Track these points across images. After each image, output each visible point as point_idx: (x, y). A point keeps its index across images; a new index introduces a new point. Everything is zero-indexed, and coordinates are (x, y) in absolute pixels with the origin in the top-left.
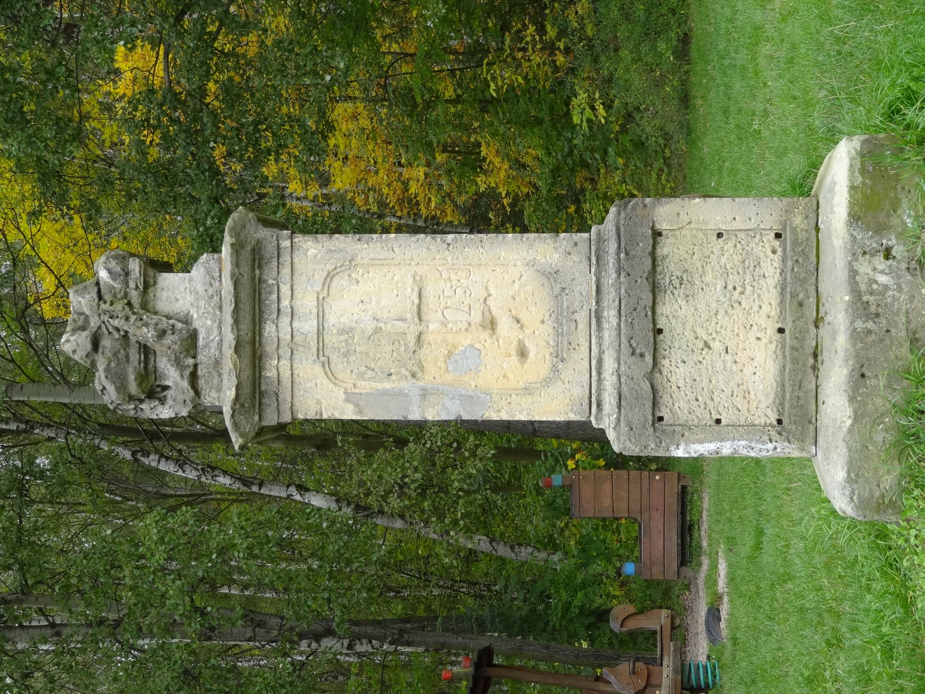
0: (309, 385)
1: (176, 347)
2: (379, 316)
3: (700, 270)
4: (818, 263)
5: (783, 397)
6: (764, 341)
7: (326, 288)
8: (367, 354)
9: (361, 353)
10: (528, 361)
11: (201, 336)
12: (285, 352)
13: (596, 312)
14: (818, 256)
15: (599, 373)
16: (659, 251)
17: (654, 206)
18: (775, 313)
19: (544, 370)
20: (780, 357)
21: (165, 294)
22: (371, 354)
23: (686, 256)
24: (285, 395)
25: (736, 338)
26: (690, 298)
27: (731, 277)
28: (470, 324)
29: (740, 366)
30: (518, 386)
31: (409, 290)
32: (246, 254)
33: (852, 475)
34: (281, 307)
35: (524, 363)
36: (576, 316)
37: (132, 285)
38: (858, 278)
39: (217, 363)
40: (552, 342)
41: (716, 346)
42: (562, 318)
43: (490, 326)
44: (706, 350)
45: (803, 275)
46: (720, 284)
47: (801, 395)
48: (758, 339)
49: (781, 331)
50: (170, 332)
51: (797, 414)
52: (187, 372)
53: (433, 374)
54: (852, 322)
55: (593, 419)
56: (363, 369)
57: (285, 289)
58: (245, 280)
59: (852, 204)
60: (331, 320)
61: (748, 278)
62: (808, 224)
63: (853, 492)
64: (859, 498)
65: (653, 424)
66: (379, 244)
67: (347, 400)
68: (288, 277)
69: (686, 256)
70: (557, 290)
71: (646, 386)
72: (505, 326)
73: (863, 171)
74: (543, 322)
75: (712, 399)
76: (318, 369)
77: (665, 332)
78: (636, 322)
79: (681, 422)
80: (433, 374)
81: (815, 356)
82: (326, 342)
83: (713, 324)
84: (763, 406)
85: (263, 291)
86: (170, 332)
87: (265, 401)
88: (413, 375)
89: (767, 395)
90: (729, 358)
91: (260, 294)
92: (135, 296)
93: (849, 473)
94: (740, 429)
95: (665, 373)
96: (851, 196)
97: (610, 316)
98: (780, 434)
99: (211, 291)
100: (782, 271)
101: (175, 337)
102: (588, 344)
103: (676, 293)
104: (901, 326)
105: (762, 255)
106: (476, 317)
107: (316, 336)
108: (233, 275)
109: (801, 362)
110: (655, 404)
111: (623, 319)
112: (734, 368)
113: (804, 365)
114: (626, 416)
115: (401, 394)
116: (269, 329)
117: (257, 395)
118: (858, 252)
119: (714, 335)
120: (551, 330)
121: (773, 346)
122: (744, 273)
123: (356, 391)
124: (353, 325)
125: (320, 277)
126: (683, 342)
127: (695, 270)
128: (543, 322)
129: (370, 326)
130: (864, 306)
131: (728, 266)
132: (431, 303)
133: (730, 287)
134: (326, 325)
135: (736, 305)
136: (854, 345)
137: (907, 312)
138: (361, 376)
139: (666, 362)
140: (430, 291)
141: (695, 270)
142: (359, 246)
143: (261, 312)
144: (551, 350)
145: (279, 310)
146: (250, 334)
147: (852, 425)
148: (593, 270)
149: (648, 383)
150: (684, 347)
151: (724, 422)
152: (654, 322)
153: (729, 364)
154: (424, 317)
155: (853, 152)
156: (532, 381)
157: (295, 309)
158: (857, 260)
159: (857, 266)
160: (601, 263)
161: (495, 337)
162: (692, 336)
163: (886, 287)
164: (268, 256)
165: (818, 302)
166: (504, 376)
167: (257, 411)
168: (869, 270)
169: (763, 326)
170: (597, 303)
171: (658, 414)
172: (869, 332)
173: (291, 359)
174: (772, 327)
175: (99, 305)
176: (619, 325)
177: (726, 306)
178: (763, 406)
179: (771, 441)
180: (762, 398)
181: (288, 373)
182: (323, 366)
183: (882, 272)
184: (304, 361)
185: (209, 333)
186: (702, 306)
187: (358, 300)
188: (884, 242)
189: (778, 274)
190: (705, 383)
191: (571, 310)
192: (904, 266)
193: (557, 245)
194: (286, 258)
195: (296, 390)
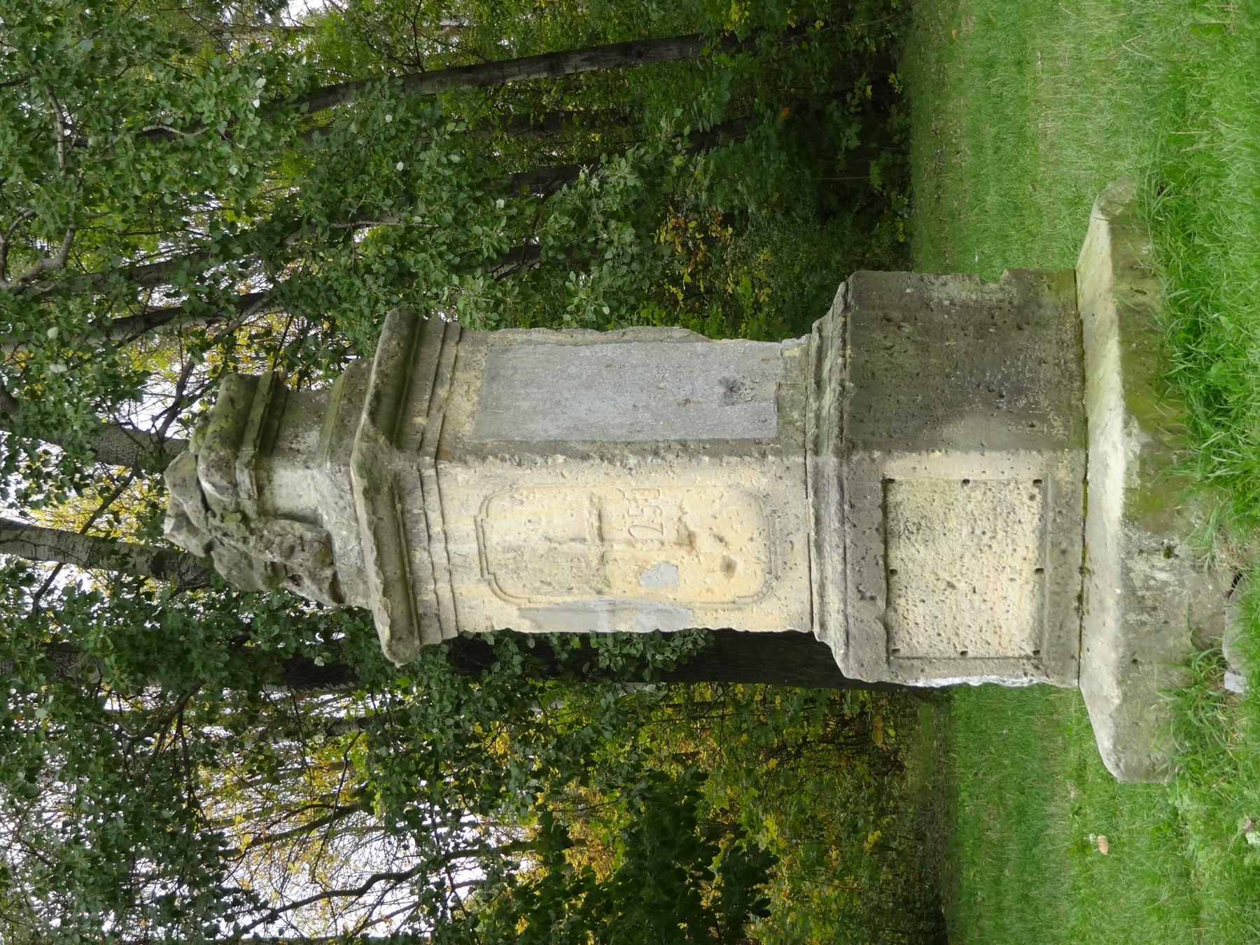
0: (474, 603)
1: (309, 564)
2: (551, 535)
3: (942, 516)
4: (1085, 514)
5: (1041, 632)
6: (1019, 582)
7: (484, 511)
8: (542, 570)
9: (533, 569)
10: (736, 575)
11: (337, 545)
12: (442, 575)
13: (816, 541)
14: (1085, 508)
15: (822, 597)
16: (891, 498)
17: (884, 460)
18: (1032, 555)
19: (755, 585)
20: (1038, 596)
21: (284, 491)
22: (546, 570)
23: (924, 503)
24: (448, 614)
25: (986, 580)
26: (930, 543)
27: (979, 522)
28: (662, 544)
29: (990, 604)
30: (726, 600)
31: (586, 513)
32: (383, 498)
33: (1119, 748)
34: (432, 532)
35: (732, 577)
36: (791, 538)
37: (243, 495)
38: (1132, 575)
39: (361, 571)
40: (763, 558)
41: (962, 586)
42: (774, 539)
43: (687, 541)
44: (950, 590)
45: (1067, 525)
46: (966, 530)
47: (1062, 634)
48: (1012, 580)
49: (1039, 571)
50: (298, 548)
51: (1058, 638)
52: (326, 585)
53: (620, 588)
54: (1124, 615)
55: (816, 630)
56: (538, 584)
57: (434, 517)
58: (387, 524)
59: (1127, 506)
60: (494, 538)
61: (1000, 524)
62: (1075, 477)
63: (1119, 759)
64: (1126, 766)
65: (888, 658)
66: (544, 470)
67: (523, 616)
68: (437, 505)
69: (924, 503)
70: (767, 511)
71: (879, 628)
72: (704, 542)
73: (1142, 474)
74: (752, 539)
75: (957, 634)
76: (484, 588)
77: (901, 573)
78: (865, 570)
79: (920, 655)
80: (620, 588)
81: (1080, 598)
82: (490, 559)
83: (958, 567)
84: (1017, 639)
85: (407, 521)
86: (298, 548)
87: (425, 622)
88: (599, 592)
89: (1022, 631)
90: (977, 598)
91: (404, 525)
92: (250, 507)
93: (1115, 745)
94: (990, 663)
95: (900, 611)
96: (1127, 498)
97: (831, 539)
98: (1037, 668)
99: (342, 503)
100: (1042, 516)
101: (306, 555)
102: (807, 564)
103: (913, 538)
104: (1182, 618)
105: (1017, 502)
106: (670, 535)
107: (477, 558)
108: (370, 523)
109: (1062, 606)
110: (889, 640)
111: (849, 566)
112: (983, 607)
113: (1067, 607)
114: (856, 653)
115: (587, 610)
116: (420, 556)
117: (415, 622)
118: (1133, 550)
119: (959, 577)
120: (761, 548)
121: (1030, 587)
122: (996, 519)
123: (532, 606)
124: (521, 543)
125: (475, 502)
126: (922, 583)
127: (935, 517)
128: (752, 539)
129: (543, 547)
130: (1136, 599)
131: (976, 513)
132: (616, 531)
133: (978, 532)
134: (488, 544)
135: (986, 549)
136: (1125, 635)
137: (1190, 605)
138: (537, 591)
139: (902, 601)
140: (613, 511)
141: (935, 517)
142: (519, 471)
143: (408, 542)
144: (763, 566)
145: (429, 536)
146: (399, 571)
147: (1120, 705)
148: (810, 500)
149: (880, 625)
150: (924, 588)
151: (971, 654)
152: (886, 565)
153: (977, 604)
154: (606, 536)
155: (1131, 455)
156: (742, 594)
157: (449, 533)
158: (1132, 558)
159: (1130, 563)
160: (821, 495)
161: (694, 553)
162: (933, 577)
163: (1166, 584)
164: (409, 486)
165: (1084, 552)
166: (708, 590)
167: (416, 635)
168: (1146, 568)
169: (1018, 567)
170: (817, 533)
171: (893, 647)
172: (1144, 624)
173: (450, 581)
174: (1028, 569)
175: (206, 519)
176: (844, 571)
177: (973, 550)
178: (1017, 639)
179: (1026, 675)
180: (1016, 632)
181: (449, 595)
182: (490, 584)
183: (1162, 569)
184: (466, 582)
185: (345, 541)
186: (944, 550)
187: (524, 519)
188: (1166, 541)
189: (1036, 519)
190: (949, 620)
191: (785, 532)
192: (1187, 563)
193: (765, 469)
194: (432, 487)
195: (459, 607)
